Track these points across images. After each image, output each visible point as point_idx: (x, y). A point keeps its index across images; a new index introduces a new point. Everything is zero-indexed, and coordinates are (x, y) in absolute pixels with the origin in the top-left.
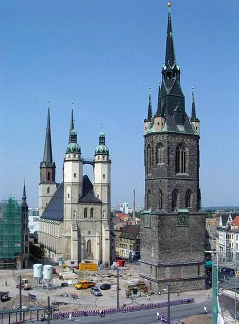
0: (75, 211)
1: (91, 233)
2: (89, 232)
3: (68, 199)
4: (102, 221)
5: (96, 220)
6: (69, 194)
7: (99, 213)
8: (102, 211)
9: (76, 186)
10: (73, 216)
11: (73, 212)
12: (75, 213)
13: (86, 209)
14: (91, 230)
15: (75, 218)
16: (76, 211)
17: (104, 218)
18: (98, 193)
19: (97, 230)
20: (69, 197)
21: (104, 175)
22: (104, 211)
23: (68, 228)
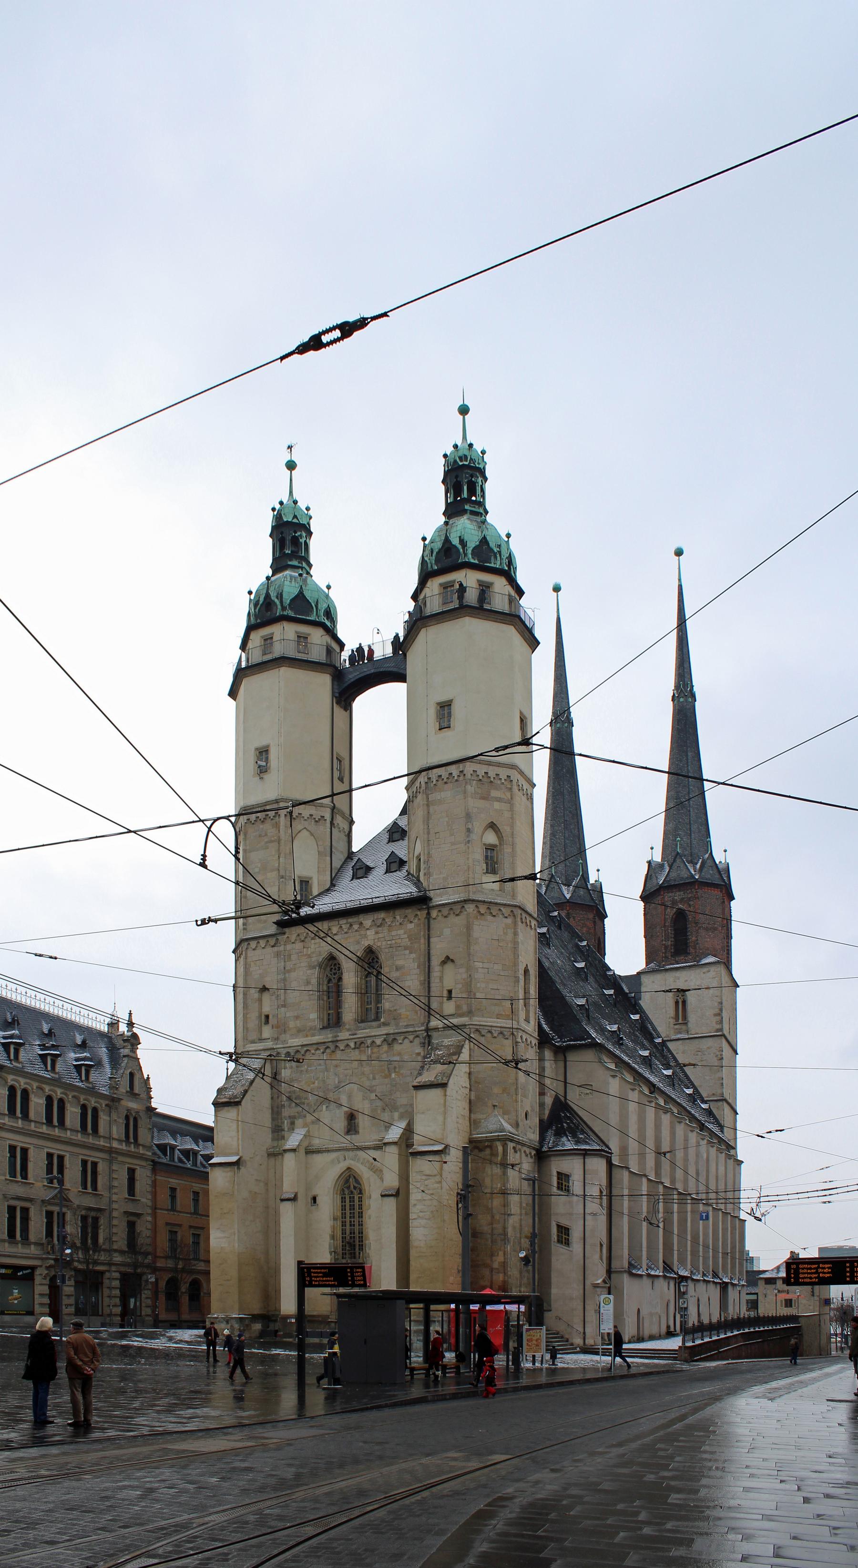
1: (363, 1122)
2: (351, 1117)
5: (390, 1030)
8: (435, 962)
11: (254, 994)
13: (331, 964)
16: (271, 981)
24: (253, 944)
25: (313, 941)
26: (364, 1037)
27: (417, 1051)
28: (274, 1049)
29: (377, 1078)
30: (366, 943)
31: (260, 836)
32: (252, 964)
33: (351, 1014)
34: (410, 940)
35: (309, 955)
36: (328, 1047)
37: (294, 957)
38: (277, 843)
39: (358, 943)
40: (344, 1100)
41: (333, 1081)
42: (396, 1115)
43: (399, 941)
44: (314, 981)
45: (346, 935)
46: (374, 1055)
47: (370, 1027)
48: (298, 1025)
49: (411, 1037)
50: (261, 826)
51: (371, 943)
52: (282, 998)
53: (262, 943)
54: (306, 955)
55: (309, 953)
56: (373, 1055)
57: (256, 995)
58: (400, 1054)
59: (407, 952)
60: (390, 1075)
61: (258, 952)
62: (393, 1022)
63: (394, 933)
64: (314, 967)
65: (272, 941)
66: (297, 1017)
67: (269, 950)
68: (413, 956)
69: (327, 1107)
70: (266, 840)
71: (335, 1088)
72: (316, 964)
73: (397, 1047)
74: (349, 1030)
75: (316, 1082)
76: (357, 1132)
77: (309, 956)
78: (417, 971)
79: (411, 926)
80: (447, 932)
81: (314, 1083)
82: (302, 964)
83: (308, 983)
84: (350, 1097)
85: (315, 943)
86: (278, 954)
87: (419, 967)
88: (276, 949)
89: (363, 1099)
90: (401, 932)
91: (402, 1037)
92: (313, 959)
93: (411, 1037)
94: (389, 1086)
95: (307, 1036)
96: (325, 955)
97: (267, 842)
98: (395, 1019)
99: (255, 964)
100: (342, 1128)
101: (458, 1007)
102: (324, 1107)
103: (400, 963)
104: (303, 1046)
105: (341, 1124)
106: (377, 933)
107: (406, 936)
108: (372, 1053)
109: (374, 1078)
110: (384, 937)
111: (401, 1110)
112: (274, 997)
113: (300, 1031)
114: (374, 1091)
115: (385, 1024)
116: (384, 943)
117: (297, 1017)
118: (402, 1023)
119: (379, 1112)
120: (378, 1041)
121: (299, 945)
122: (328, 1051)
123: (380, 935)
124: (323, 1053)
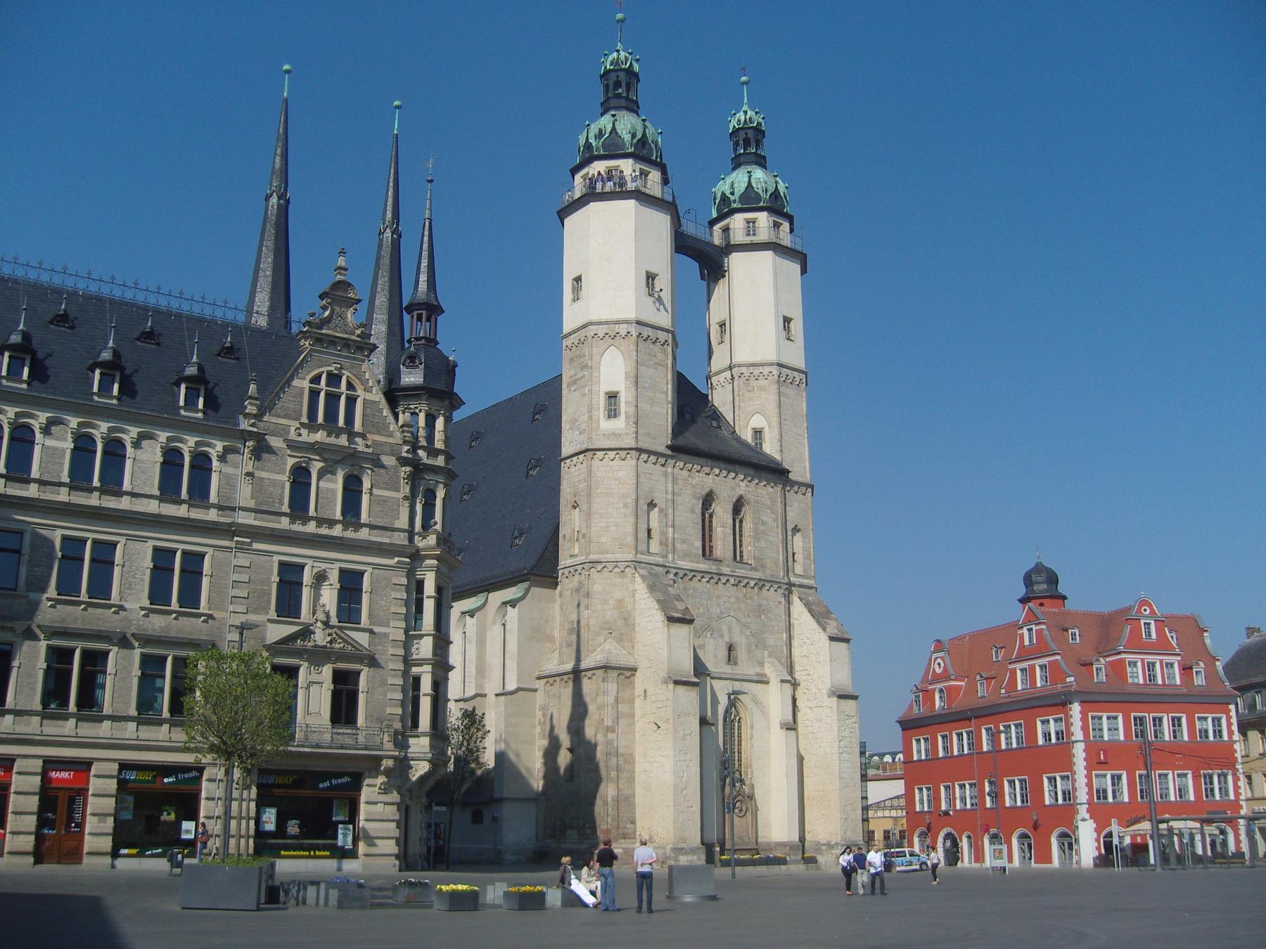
0: (652, 505)
1: (741, 654)
2: (730, 648)
3: (606, 425)
4: (791, 585)
6: (612, 396)
7: (776, 537)
8: (790, 527)
9: (657, 347)
10: (643, 534)
12: (655, 514)
14: (741, 640)
15: (655, 547)
16: (659, 498)
17: (799, 569)
18: (757, 422)
19: (770, 642)
20: (612, 413)
21: (787, 321)
22: (796, 530)
23: (611, 614)
24: (644, 456)
25: (697, 473)
26: (743, 577)
27: (779, 600)
28: (665, 566)
29: (751, 615)
30: (740, 492)
31: (650, 355)
32: (642, 474)
33: (729, 552)
34: (771, 502)
35: (694, 485)
36: (712, 578)
37: (680, 482)
38: (664, 369)
39: (733, 489)
40: (725, 629)
41: (715, 610)
42: (766, 653)
43: (763, 499)
44: (699, 511)
45: (724, 479)
46: (747, 595)
47: (744, 569)
48: (685, 548)
49: (776, 586)
50: (652, 346)
51: (744, 494)
52: (670, 517)
53: (653, 458)
54: (691, 484)
55: (694, 483)
56: (747, 595)
57: (646, 507)
58: (766, 599)
59: (769, 511)
60: (760, 617)
61: (649, 464)
62: (761, 569)
63: (759, 491)
64: (698, 498)
65: (662, 460)
66: (684, 541)
67: (658, 467)
68: (773, 516)
69: (711, 634)
70: (656, 361)
71: (718, 617)
72: (700, 495)
73: (764, 590)
74: (728, 566)
75: (701, 608)
76: (736, 663)
77: (694, 486)
78: (775, 530)
79: (772, 490)
80: (796, 504)
81: (699, 608)
82: (688, 492)
83: (693, 511)
84: (730, 629)
85: (699, 476)
86: (666, 474)
87: (778, 527)
88: (664, 469)
89: (741, 634)
90: (764, 492)
91: (769, 585)
92: (697, 491)
93: (776, 586)
94: (760, 625)
95: (692, 562)
96: (707, 490)
97: (656, 364)
98: (762, 567)
99: (645, 476)
100: (724, 657)
101: (805, 570)
102: (709, 634)
103: (765, 519)
104: (691, 571)
105: (723, 653)
106: (747, 486)
107: (768, 497)
108: (747, 593)
109: (749, 616)
110: (752, 492)
111: (770, 649)
112: (662, 514)
113: (686, 555)
114: (750, 628)
115: (755, 569)
116: (753, 497)
117: (684, 541)
118: (768, 572)
119: (753, 647)
120: (752, 583)
121: (685, 473)
122: (712, 581)
123: (750, 489)
124: (708, 582)
